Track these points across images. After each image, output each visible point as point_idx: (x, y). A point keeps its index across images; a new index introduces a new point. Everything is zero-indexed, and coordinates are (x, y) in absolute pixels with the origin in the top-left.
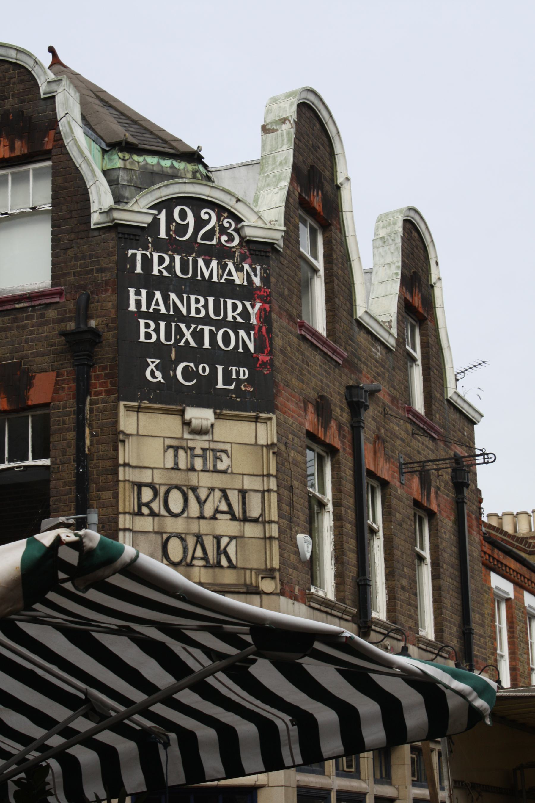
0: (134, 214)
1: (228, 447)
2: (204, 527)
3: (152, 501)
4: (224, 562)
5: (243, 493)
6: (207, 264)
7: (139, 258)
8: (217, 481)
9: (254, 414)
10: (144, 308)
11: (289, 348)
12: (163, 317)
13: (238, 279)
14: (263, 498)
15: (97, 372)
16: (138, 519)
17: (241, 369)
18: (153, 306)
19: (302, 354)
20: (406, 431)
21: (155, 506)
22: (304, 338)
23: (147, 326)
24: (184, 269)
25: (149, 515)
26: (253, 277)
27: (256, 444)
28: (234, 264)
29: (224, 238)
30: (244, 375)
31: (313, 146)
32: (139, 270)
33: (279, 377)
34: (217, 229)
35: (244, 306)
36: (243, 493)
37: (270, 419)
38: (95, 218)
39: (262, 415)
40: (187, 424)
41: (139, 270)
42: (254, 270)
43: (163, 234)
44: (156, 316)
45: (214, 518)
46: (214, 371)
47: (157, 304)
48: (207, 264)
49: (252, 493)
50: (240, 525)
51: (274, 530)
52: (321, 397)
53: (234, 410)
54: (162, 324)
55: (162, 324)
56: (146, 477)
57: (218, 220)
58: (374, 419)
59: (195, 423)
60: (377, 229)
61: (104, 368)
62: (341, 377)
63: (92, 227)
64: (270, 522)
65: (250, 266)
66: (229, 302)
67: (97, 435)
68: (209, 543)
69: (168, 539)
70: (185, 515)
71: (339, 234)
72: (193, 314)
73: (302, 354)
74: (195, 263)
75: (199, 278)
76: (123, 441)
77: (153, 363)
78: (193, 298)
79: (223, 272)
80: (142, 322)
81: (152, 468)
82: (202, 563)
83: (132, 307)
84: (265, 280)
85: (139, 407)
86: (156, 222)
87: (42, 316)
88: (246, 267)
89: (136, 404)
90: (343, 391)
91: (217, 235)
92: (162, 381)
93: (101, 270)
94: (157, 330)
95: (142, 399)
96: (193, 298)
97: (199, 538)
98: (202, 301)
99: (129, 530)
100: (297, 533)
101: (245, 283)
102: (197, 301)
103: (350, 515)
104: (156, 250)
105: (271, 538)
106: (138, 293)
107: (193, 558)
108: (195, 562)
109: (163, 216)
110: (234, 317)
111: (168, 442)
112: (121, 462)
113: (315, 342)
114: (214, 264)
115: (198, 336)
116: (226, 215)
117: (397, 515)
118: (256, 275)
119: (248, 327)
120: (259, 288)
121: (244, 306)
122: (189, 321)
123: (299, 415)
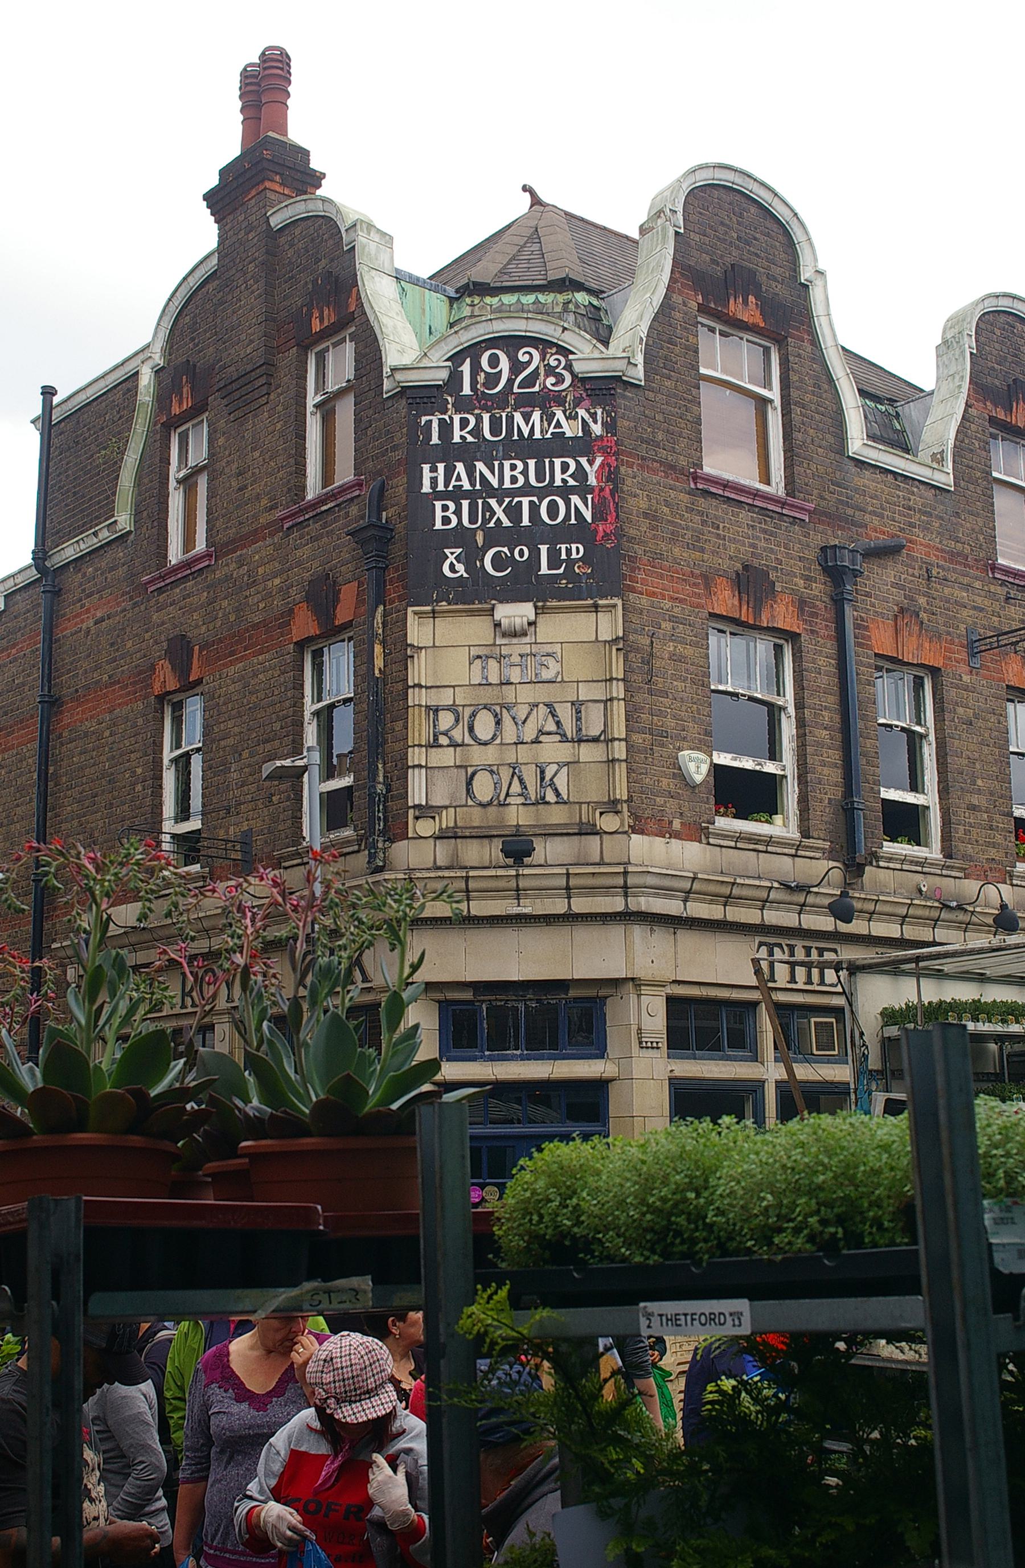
0: (427, 371)
1: (557, 648)
2: (524, 753)
3: (452, 728)
4: (550, 797)
5: (577, 706)
6: (527, 418)
7: (435, 425)
8: (542, 694)
9: (590, 602)
10: (441, 487)
11: (666, 510)
12: (466, 495)
13: (570, 430)
14: (605, 708)
15: (392, 575)
16: (433, 751)
17: (574, 546)
18: (453, 483)
19: (701, 513)
20: (991, 596)
21: (457, 734)
22: (706, 493)
23: (445, 508)
24: (495, 430)
25: (448, 746)
26: (592, 424)
27: (597, 640)
28: (564, 412)
29: (551, 380)
30: (578, 553)
31: (739, 238)
32: (435, 440)
33: (639, 550)
34: (542, 371)
35: (578, 463)
36: (577, 706)
37: (614, 606)
38: (387, 385)
39: (600, 602)
40: (497, 625)
41: (435, 440)
42: (594, 416)
43: (467, 390)
44: (457, 495)
45: (536, 741)
46: (535, 554)
47: (459, 479)
48: (527, 418)
49: (590, 704)
50: (574, 747)
51: (620, 750)
52: (746, 567)
53: (565, 600)
54: (465, 504)
55: (465, 504)
56: (446, 698)
57: (543, 359)
58: (895, 585)
59: (505, 622)
60: (944, 332)
61: (397, 570)
62: (807, 535)
63: (385, 396)
64: (613, 740)
65: (588, 411)
66: (558, 462)
67: (390, 654)
68: (530, 776)
69: (474, 774)
70: (498, 741)
71: (809, 348)
72: (507, 484)
73: (701, 513)
74: (510, 419)
75: (516, 437)
76: (412, 657)
77: (452, 554)
78: (507, 464)
79: (549, 425)
80: (438, 505)
81: (454, 687)
82: (520, 800)
83: (426, 488)
84: (610, 426)
85: (433, 612)
86: (455, 377)
87: (347, 514)
88: (582, 412)
89: (429, 608)
90: (812, 554)
91: (542, 377)
92: (465, 575)
93: (394, 448)
94: (458, 512)
95: (438, 601)
96: (507, 464)
97: (514, 768)
98: (520, 466)
99: (420, 766)
100: (680, 749)
101: (580, 434)
102: (513, 467)
103: (830, 717)
104: (458, 411)
105: (613, 760)
106: (433, 470)
107: (507, 795)
108: (509, 800)
109: (466, 368)
110: (564, 481)
111: (475, 651)
112: (410, 683)
113: (733, 496)
114: (536, 416)
115: (513, 511)
116: (554, 350)
117: (960, 710)
118: (595, 422)
119: (583, 490)
120: (600, 438)
121: (578, 463)
122: (499, 494)
123: (698, 596)
